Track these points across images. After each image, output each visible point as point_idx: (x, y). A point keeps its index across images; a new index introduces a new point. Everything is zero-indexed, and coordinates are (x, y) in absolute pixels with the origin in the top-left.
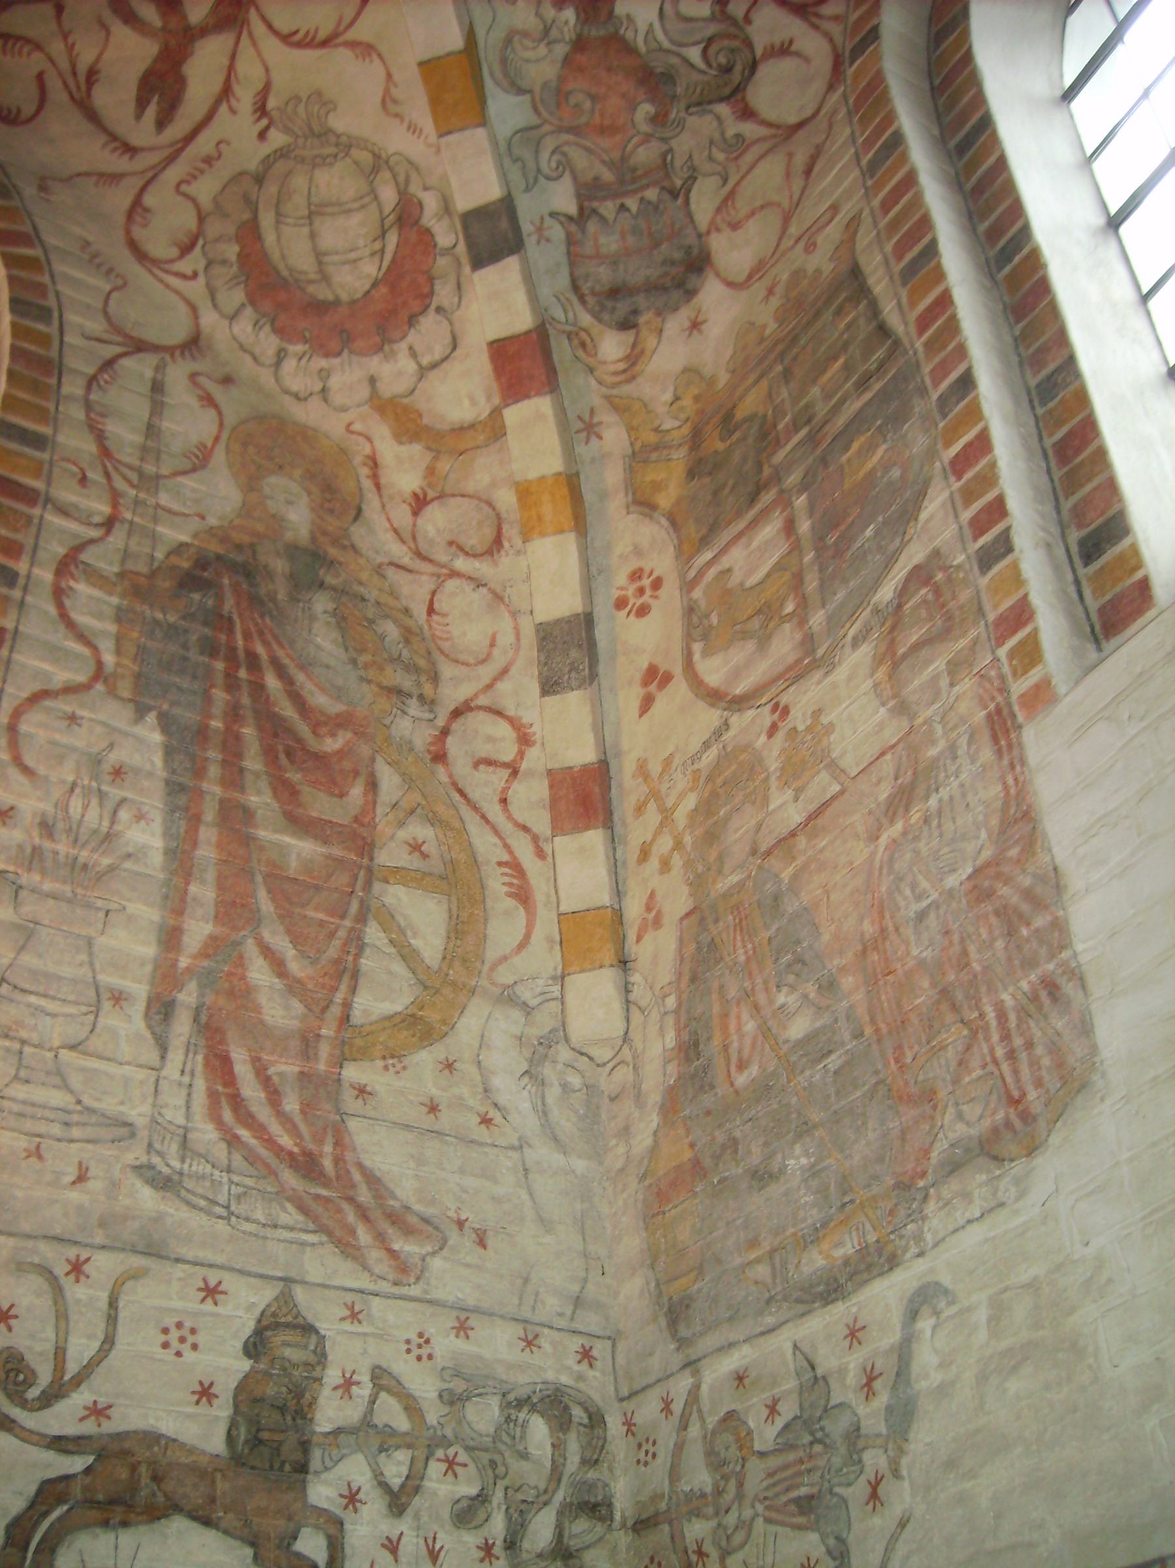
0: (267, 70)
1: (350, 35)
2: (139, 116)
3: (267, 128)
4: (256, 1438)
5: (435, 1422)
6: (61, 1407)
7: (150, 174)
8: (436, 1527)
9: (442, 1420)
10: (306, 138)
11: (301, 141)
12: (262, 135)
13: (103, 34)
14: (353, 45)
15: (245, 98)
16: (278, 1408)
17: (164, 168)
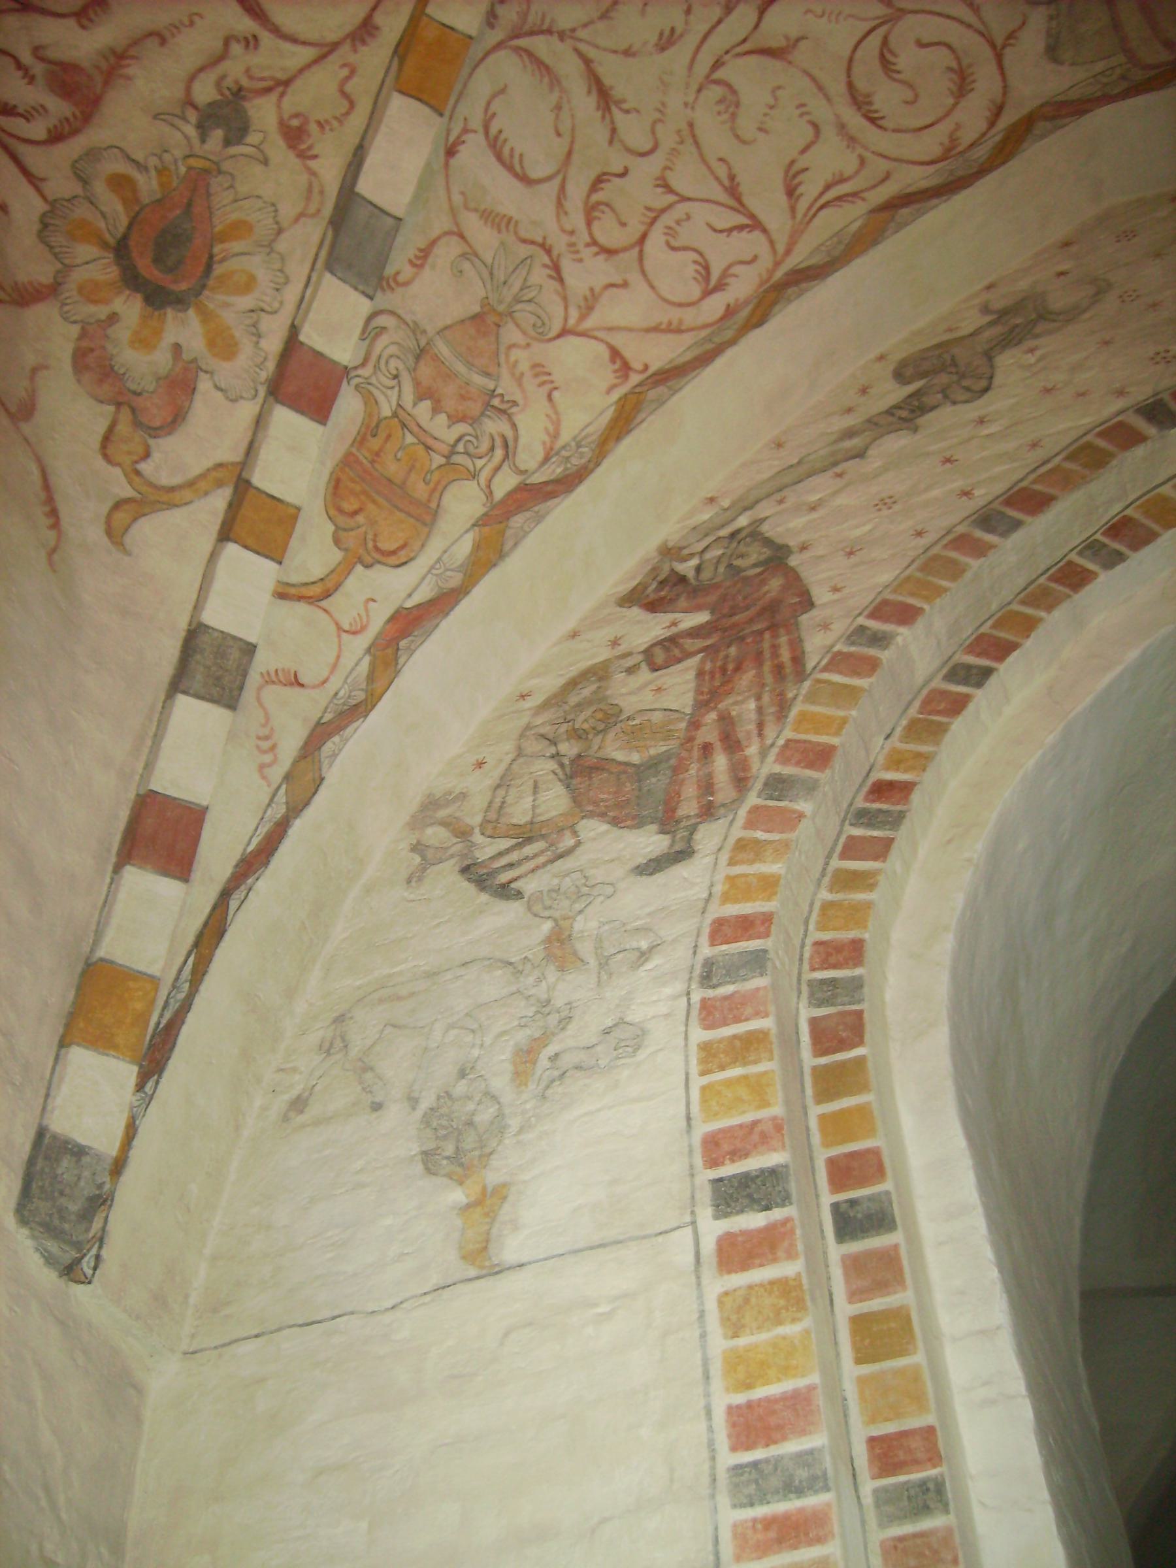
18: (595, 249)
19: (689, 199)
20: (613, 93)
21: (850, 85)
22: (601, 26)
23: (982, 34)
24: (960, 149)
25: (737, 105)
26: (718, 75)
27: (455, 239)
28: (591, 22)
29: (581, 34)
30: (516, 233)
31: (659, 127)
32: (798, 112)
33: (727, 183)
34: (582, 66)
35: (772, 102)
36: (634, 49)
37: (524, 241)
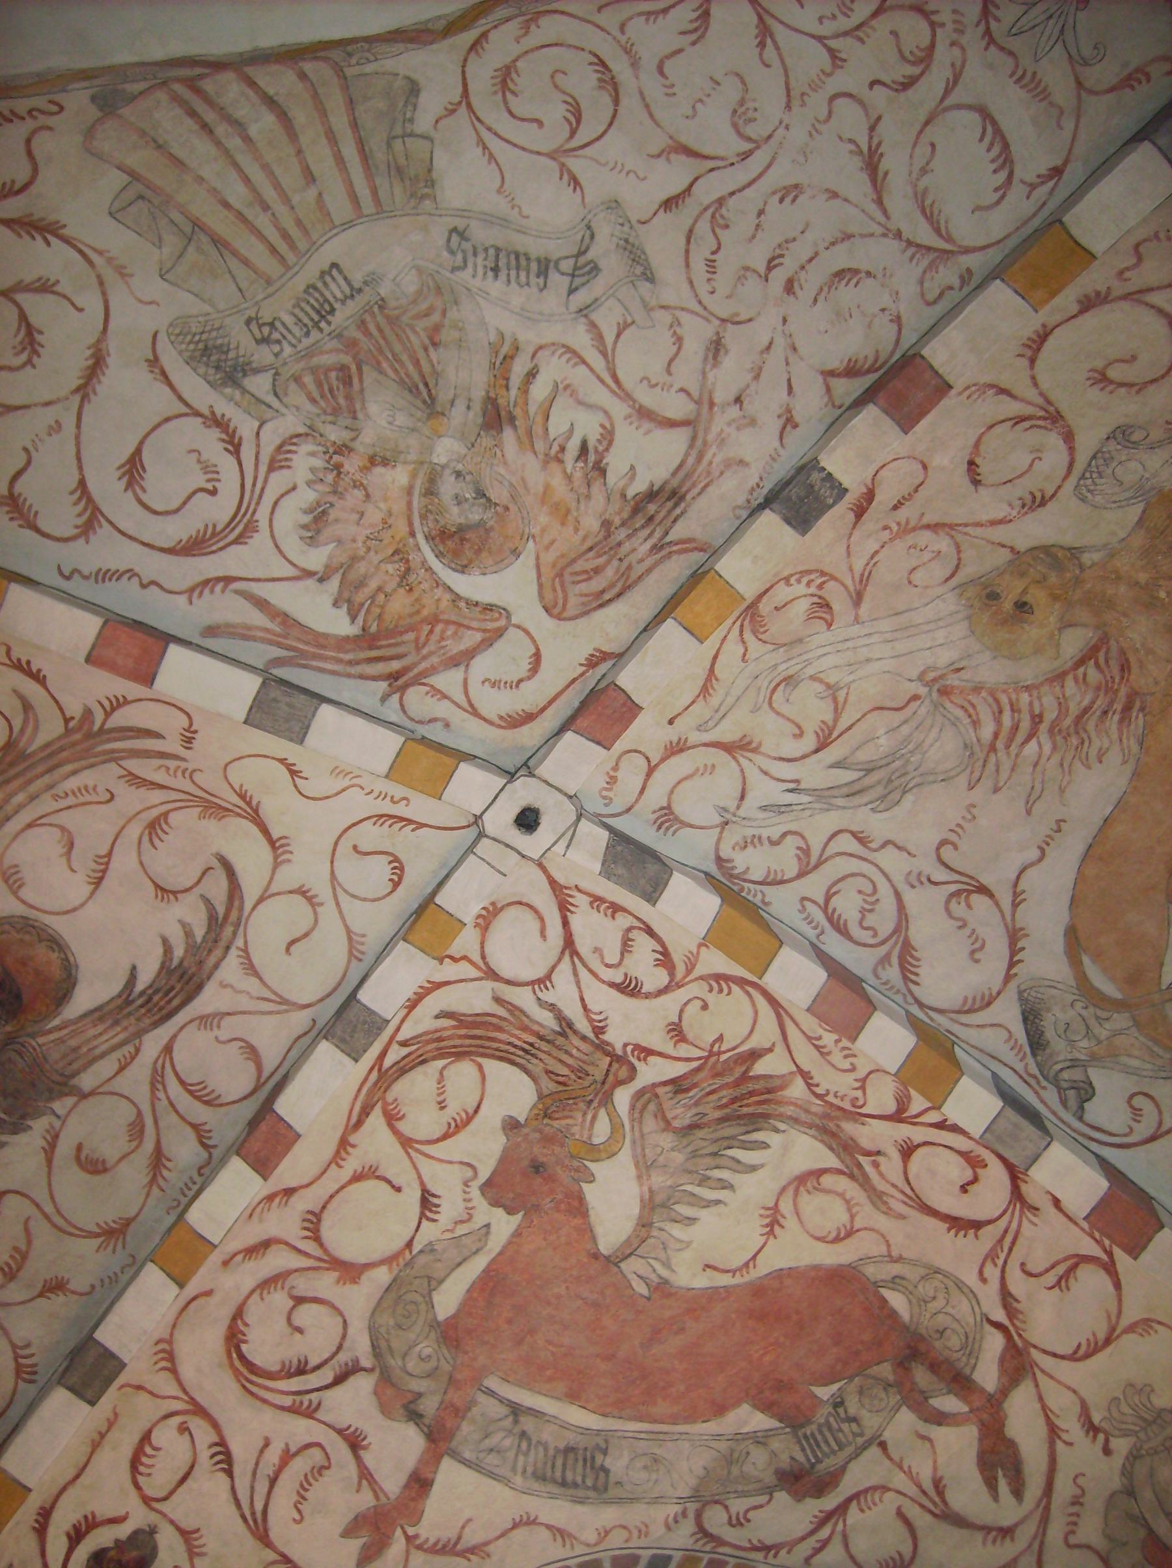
0: (1075, 1392)
1: (1125, 1322)
2: (996, 1498)
3: (1107, 1441)
7: (1036, 1546)
10: (1144, 1429)
11: (1142, 1435)
12: (1107, 1451)
13: (927, 1445)
14: (1131, 1329)
15: (1071, 1426)
17: (1044, 1534)
18: (934, 18)
19: (813, 36)
20: (860, 164)
21: (616, 101)
22: (852, 229)
23: (478, 119)
24: (521, 19)
25: (735, 111)
26: (749, 146)
27: (1087, 84)
28: (862, 236)
29: (879, 230)
30: (1017, 66)
31: (822, 117)
32: (675, 90)
33: (769, 41)
34: (885, 201)
35: (699, 106)
36: (826, 196)
37: (1011, 54)
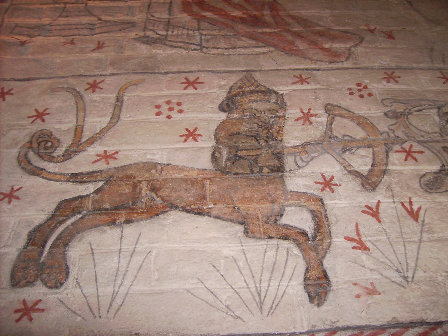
4: (236, 155)
5: (386, 129)
6: (79, 157)
8: (409, 194)
9: (392, 128)
16: (252, 136)
